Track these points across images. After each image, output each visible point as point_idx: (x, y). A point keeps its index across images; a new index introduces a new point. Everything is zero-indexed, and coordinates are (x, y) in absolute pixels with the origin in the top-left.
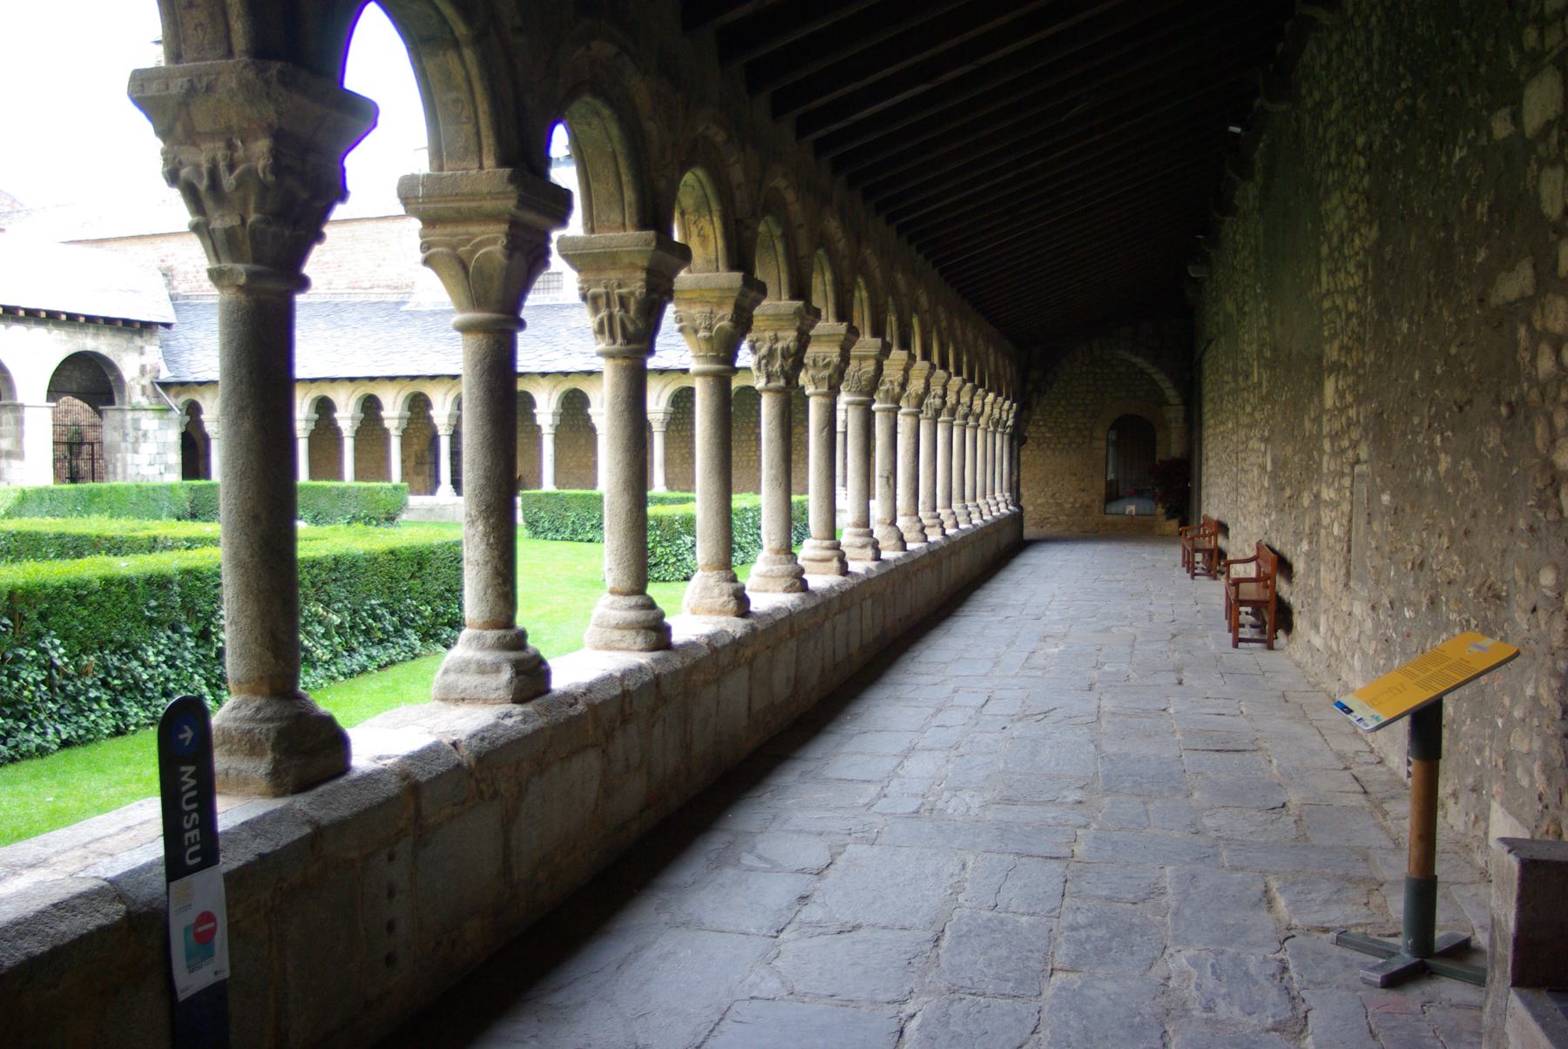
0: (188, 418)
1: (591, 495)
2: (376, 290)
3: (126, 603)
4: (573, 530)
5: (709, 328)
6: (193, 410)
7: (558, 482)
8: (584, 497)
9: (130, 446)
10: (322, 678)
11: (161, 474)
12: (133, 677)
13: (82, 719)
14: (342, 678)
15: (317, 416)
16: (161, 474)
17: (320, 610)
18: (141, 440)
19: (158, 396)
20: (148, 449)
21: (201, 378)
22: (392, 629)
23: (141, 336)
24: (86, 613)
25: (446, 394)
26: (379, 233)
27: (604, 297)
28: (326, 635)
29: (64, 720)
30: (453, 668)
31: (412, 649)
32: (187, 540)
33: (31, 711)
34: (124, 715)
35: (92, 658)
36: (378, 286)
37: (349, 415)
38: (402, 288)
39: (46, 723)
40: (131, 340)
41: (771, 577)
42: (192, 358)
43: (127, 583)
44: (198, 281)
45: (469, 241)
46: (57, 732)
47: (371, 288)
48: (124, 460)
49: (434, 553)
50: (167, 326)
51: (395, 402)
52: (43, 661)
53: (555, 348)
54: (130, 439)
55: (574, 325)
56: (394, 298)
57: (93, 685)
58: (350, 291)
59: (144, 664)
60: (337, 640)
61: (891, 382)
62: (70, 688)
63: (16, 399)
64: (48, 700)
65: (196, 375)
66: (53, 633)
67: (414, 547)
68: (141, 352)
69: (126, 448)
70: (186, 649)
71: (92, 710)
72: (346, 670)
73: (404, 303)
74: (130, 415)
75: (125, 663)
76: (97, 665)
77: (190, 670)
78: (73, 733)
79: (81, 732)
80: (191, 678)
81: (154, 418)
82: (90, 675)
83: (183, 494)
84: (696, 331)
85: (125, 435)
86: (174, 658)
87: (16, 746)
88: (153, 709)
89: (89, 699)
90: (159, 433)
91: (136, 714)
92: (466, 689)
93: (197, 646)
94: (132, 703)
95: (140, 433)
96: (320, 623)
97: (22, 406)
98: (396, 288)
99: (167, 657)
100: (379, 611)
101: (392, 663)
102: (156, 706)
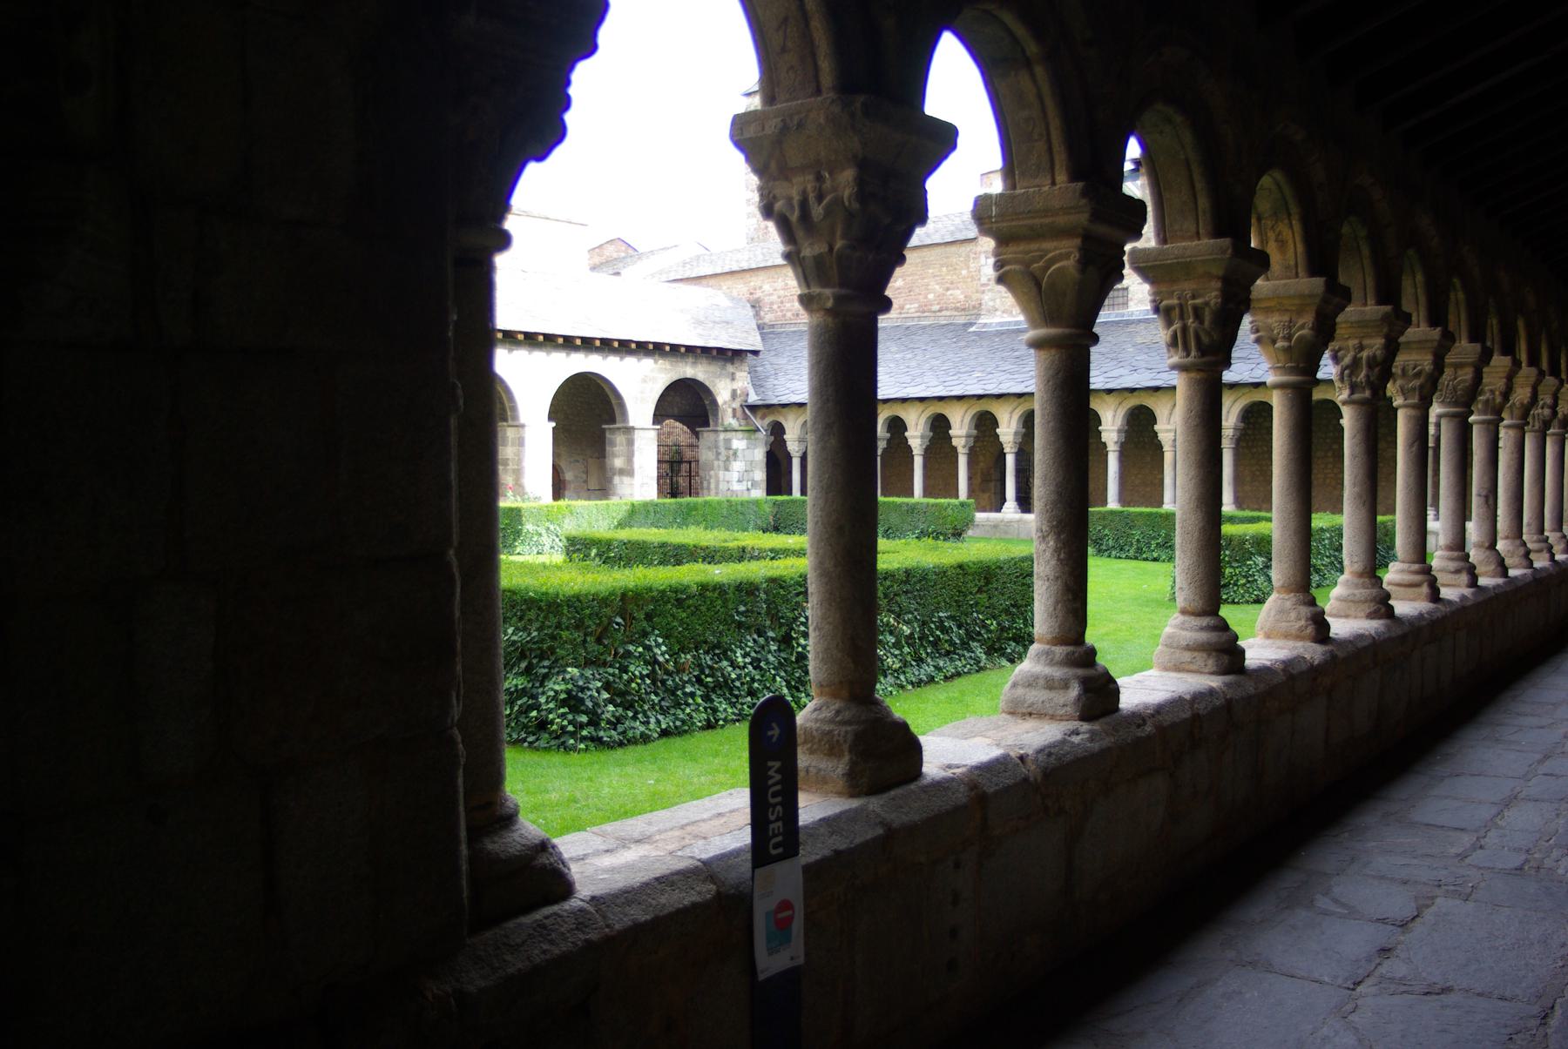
0: (772, 438)
1: (1157, 513)
2: (944, 313)
3: (718, 607)
4: (1138, 548)
5: (1288, 338)
6: (777, 430)
7: (1123, 500)
8: (1150, 515)
9: (721, 464)
10: (891, 686)
11: (748, 490)
12: (723, 674)
13: (679, 712)
14: (910, 687)
15: (888, 435)
16: (748, 490)
17: (891, 620)
18: (732, 458)
19: (746, 417)
20: (737, 466)
21: (784, 400)
22: (958, 642)
23: (733, 364)
24: (684, 615)
25: (1011, 413)
26: (947, 257)
27: (1177, 310)
28: (897, 645)
29: (664, 712)
30: (1021, 682)
31: (978, 662)
32: (772, 550)
33: (637, 702)
34: (715, 710)
35: (688, 657)
36: (947, 309)
37: (963, 432)
39: (649, 713)
40: (723, 368)
41: (1352, 601)
42: (776, 382)
43: (720, 589)
44: (782, 311)
45: (1041, 257)
46: (658, 722)
47: (940, 311)
48: (717, 476)
49: (1001, 568)
50: (755, 353)
51: (962, 421)
52: (648, 657)
53: (1121, 364)
54: (722, 458)
55: (1139, 340)
56: (962, 320)
57: (689, 681)
59: (733, 665)
60: (906, 650)
61: (1492, 392)
62: (670, 682)
64: (651, 692)
65: (779, 399)
66: (657, 632)
67: (981, 562)
69: (719, 466)
70: (770, 652)
71: (688, 705)
72: (914, 680)
73: (971, 324)
74: (722, 436)
75: (717, 663)
76: (693, 663)
77: (773, 672)
78: (671, 724)
79: (678, 723)
80: (774, 680)
81: (743, 439)
82: (687, 672)
83: (767, 509)
84: (1274, 342)
85: (718, 454)
86: (759, 661)
87: (624, 732)
88: (739, 707)
89: (685, 694)
90: (747, 452)
91: (725, 710)
92: (1033, 704)
93: (779, 650)
94: (722, 700)
95: (731, 452)
96: (891, 633)
97: (633, 428)
99: (753, 658)
100: (946, 624)
101: (958, 674)
102: (742, 704)
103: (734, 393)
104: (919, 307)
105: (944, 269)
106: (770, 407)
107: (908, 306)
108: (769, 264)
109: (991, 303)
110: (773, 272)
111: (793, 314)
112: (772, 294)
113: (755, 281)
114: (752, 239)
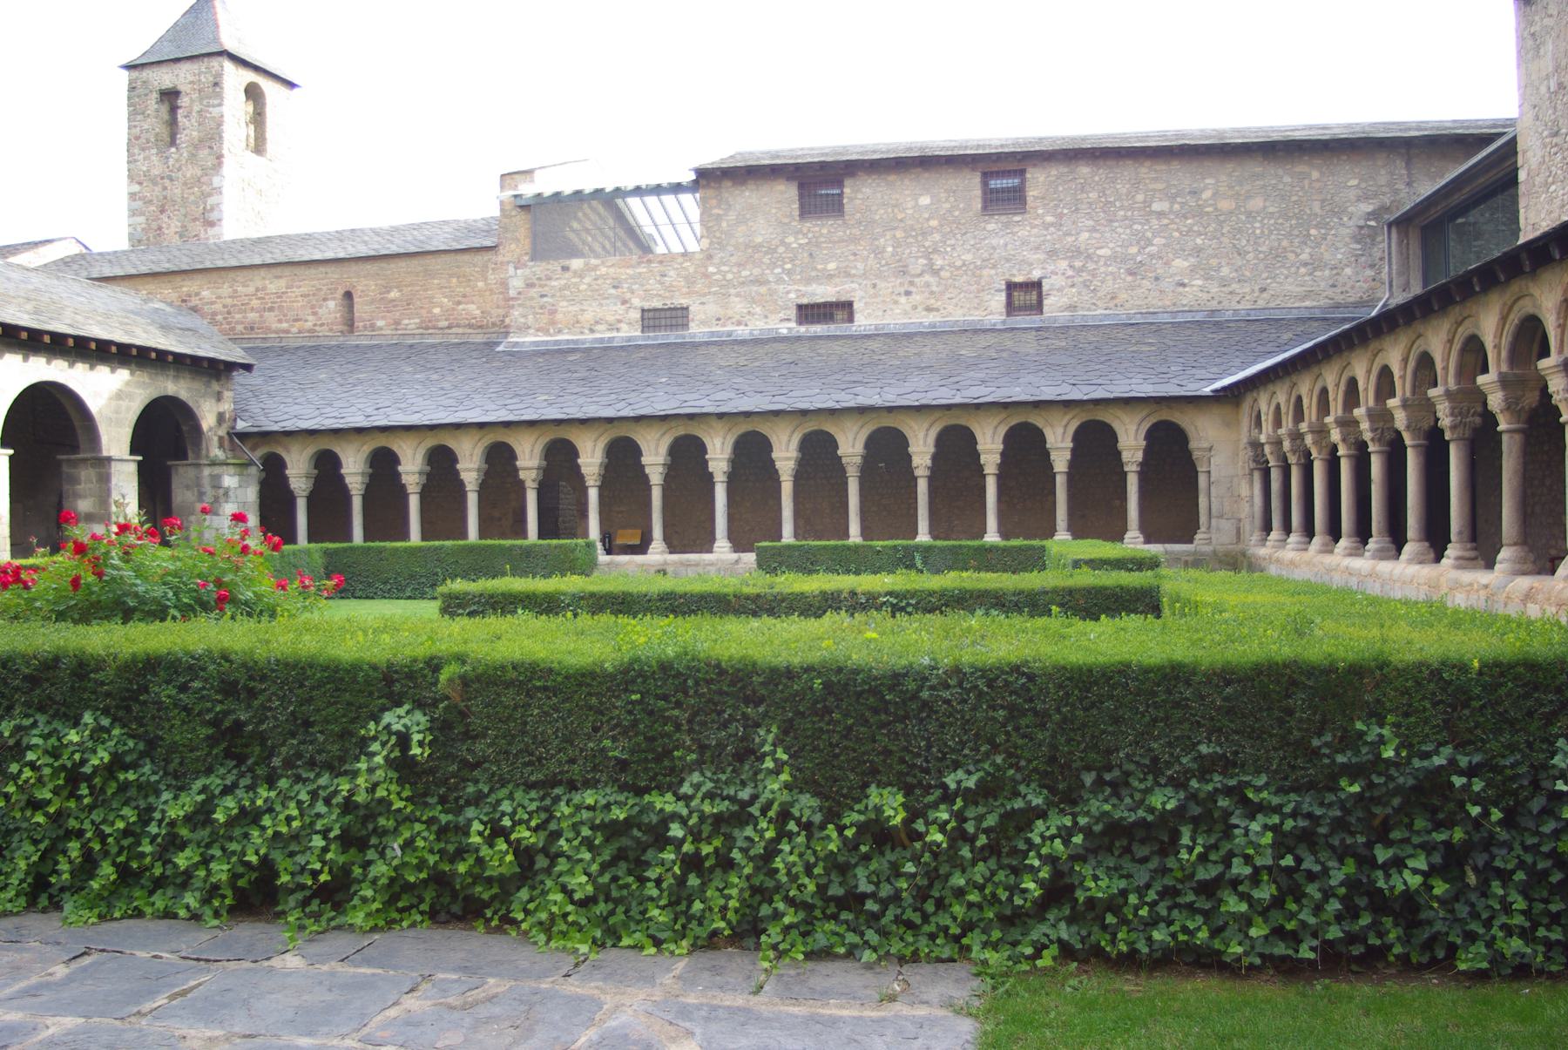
0: (264, 474)
2: (454, 330)
7: (866, 532)
8: (835, 548)
18: (222, 499)
19: (233, 448)
21: (290, 425)
23: (218, 380)
36: (458, 326)
38: (487, 327)
40: (208, 385)
44: (229, 323)
47: (449, 327)
53: (721, 387)
56: (479, 339)
58: (421, 331)
63: (100, 450)
68: (219, 397)
74: (207, 471)
83: (318, 560)
85: (201, 494)
90: (239, 492)
97: (109, 459)
98: (481, 327)
103: (221, 418)
104: (422, 322)
105: (454, 280)
106: (266, 436)
107: (406, 322)
108: (208, 265)
109: (522, 320)
110: (214, 275)
111: (245, 328)
112: (212, 303)
113: (189, 286)
114: (139, 241)
